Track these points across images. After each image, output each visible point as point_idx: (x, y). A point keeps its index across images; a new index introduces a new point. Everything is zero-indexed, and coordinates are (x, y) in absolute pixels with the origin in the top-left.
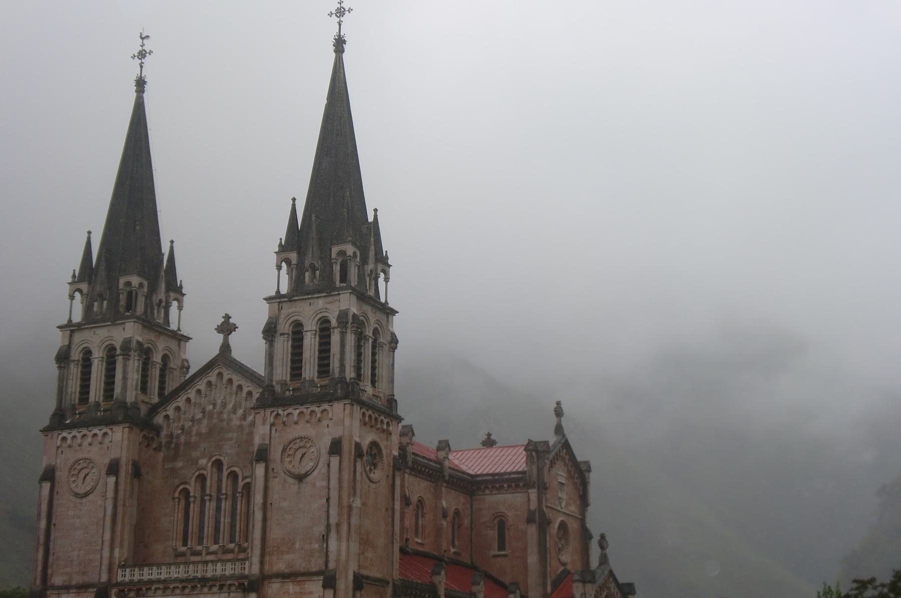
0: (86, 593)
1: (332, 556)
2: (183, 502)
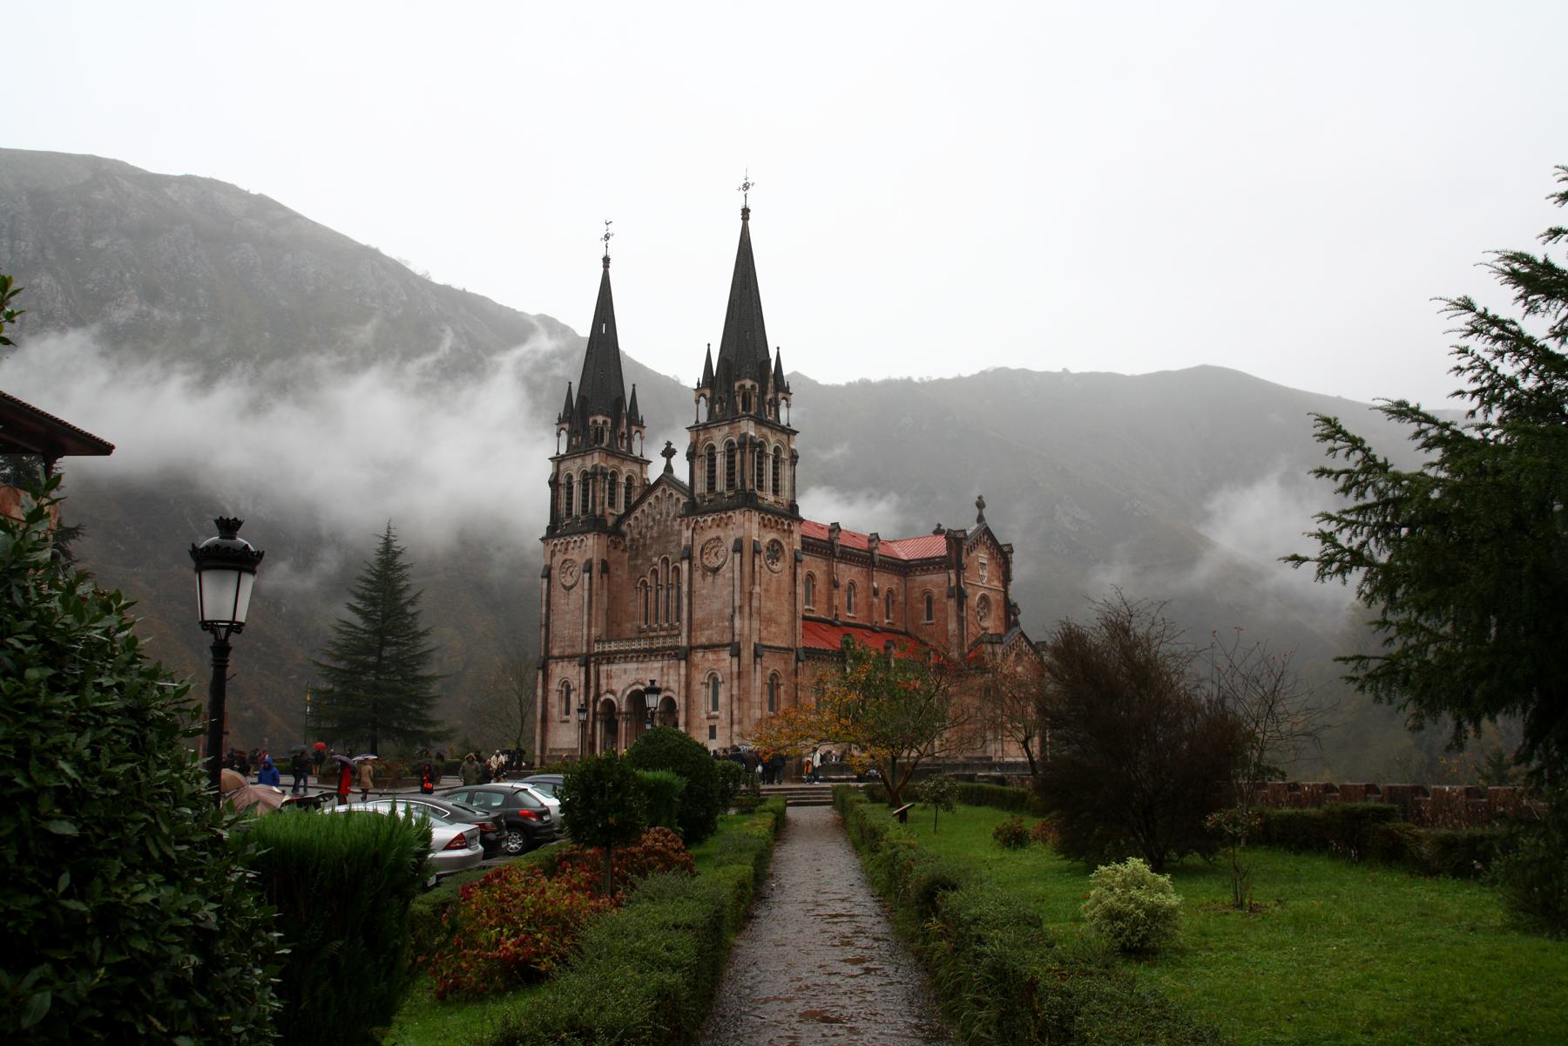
1: (737, 631)
2: (644, 590)
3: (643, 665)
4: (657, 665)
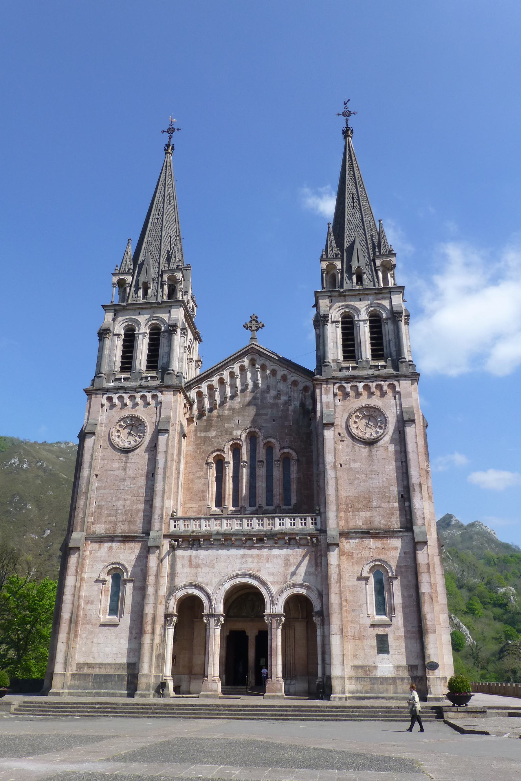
3: (255, 552)
4: (276, 552)
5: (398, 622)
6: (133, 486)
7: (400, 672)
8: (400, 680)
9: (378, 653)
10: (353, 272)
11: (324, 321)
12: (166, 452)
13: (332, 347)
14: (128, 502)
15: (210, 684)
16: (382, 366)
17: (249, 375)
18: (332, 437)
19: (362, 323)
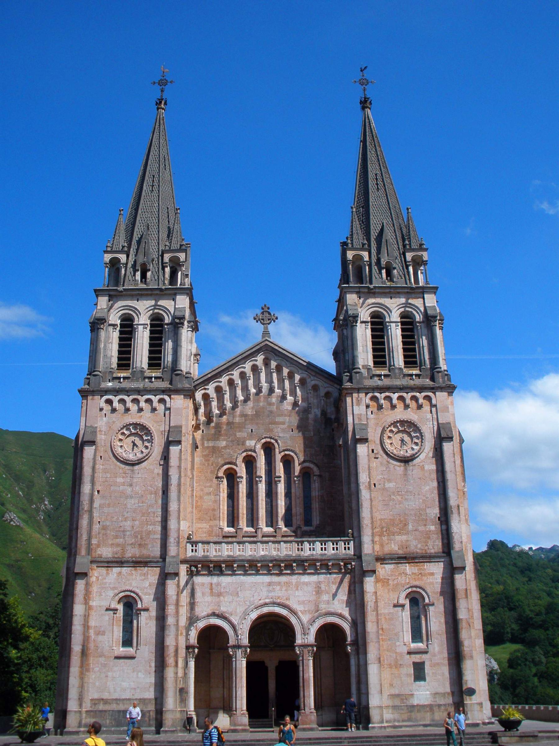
0: (146, 568)
3: (283, 579)
4: (306, 579)
5: (434, 649)
6: (141, 505)
7: (437, 699)
8: (437, 707)
9: (415, 681)
10: (382, 266)
11: (353, 322)
12: (179, 467)
13: (361, 351)
14: (137, 523)
15: (239, 718)
16: (416, 375)
17: (263, 376)
18: (366, 454)
19: (393, 325)
